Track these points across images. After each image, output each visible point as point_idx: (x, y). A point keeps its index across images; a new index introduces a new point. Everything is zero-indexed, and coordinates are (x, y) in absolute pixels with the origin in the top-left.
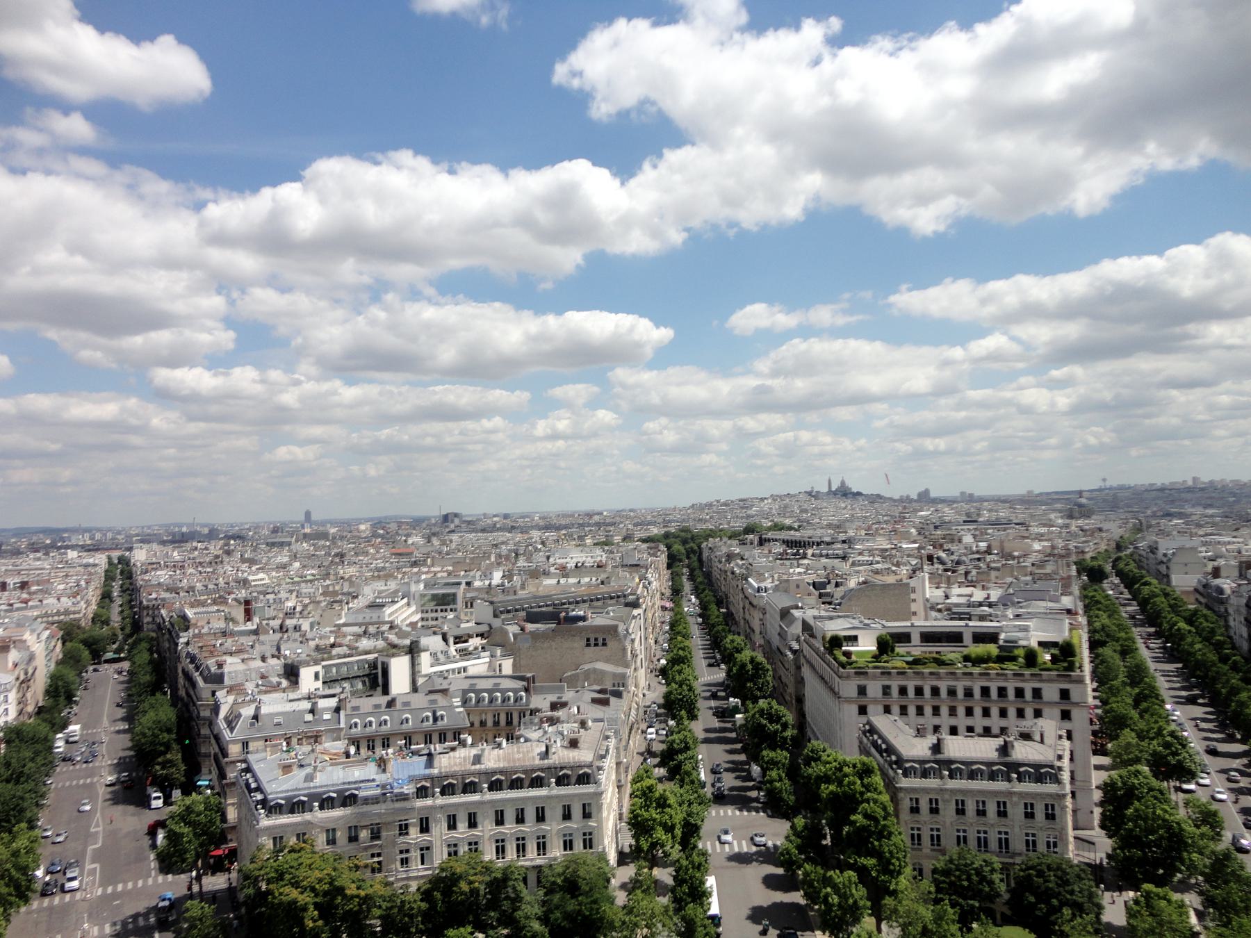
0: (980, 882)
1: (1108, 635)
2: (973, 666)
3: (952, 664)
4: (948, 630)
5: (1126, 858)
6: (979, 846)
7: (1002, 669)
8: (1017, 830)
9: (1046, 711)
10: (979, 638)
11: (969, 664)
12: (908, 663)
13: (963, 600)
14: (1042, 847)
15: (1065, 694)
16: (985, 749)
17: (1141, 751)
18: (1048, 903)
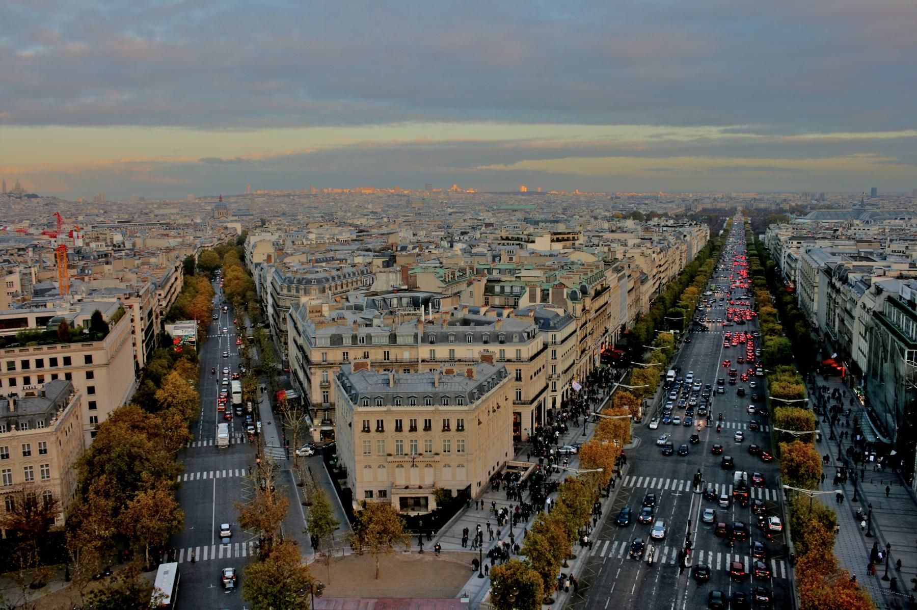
14: (38, 477)
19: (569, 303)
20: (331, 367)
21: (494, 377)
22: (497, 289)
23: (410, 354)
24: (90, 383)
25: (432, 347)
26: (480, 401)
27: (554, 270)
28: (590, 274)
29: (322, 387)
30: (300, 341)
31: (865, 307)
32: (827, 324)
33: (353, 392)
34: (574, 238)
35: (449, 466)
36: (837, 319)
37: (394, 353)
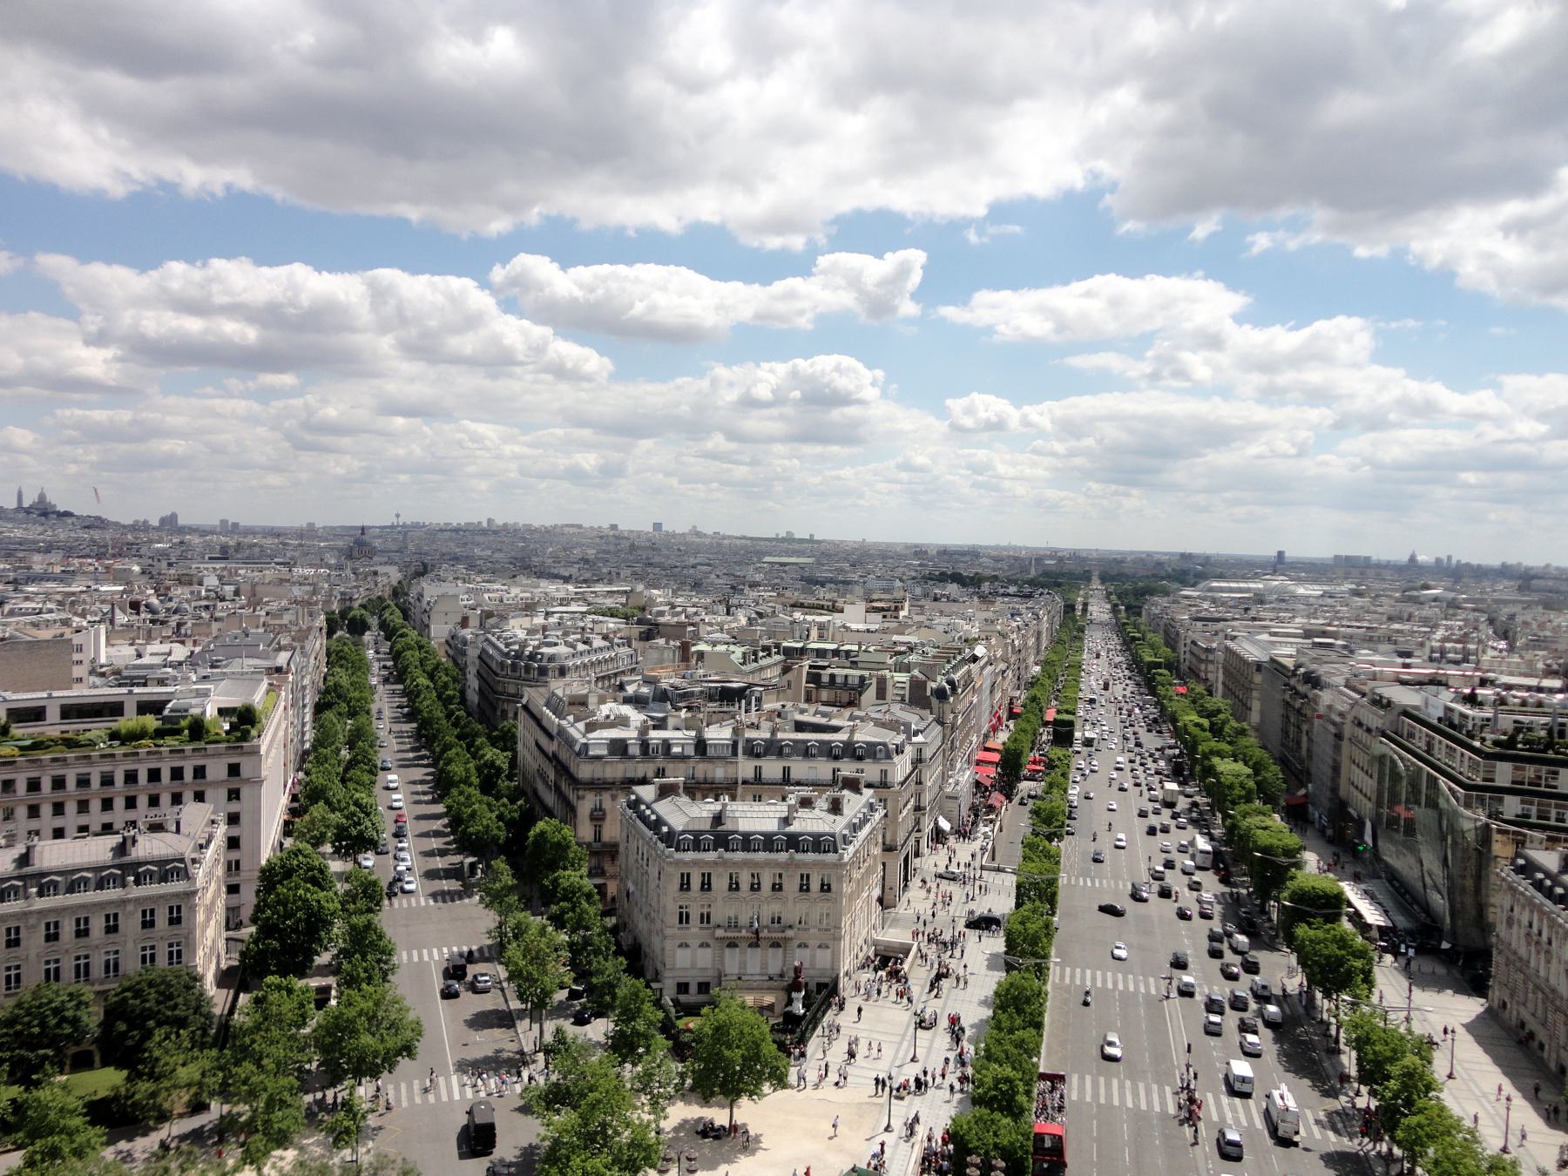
0: (58, 1025)
1: (339, 697)
2: (123, 744)
3: (92, 744)
4: (102, 700)
5: (260, 952)
6: (78, 975)
7: (156, 745)
8: (130, 945)
9: (209, 794)
10: (144, 708)
11: (117, 743)
12: (22, 748)
13: (157, 660)
14: (162, 961)
15: (234, 770)
16: (98, 850)
17: (328, 827)
18: (142, 1027)
19: (935, 701)
20: (608, 789)
21: (865, 810)
22: (825, 679)
23: (726, 772)
24: (234, 807)
25: (757, 763)
26: (851, 849)
27: (901, 653)
28: (954, 662)
29: (593, 818)
30: (551, 747)
31: (1360, 724)
32: (1283, 745)
33: (665, 829)
34: (896, 607)
35: (806, 946)
36: (1305, 738)
37: (702, 769)
